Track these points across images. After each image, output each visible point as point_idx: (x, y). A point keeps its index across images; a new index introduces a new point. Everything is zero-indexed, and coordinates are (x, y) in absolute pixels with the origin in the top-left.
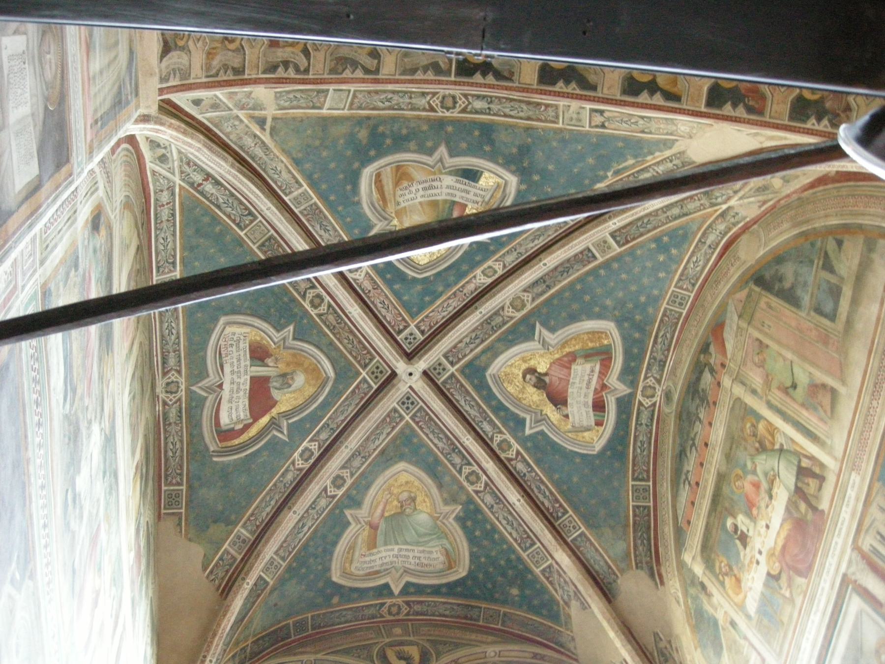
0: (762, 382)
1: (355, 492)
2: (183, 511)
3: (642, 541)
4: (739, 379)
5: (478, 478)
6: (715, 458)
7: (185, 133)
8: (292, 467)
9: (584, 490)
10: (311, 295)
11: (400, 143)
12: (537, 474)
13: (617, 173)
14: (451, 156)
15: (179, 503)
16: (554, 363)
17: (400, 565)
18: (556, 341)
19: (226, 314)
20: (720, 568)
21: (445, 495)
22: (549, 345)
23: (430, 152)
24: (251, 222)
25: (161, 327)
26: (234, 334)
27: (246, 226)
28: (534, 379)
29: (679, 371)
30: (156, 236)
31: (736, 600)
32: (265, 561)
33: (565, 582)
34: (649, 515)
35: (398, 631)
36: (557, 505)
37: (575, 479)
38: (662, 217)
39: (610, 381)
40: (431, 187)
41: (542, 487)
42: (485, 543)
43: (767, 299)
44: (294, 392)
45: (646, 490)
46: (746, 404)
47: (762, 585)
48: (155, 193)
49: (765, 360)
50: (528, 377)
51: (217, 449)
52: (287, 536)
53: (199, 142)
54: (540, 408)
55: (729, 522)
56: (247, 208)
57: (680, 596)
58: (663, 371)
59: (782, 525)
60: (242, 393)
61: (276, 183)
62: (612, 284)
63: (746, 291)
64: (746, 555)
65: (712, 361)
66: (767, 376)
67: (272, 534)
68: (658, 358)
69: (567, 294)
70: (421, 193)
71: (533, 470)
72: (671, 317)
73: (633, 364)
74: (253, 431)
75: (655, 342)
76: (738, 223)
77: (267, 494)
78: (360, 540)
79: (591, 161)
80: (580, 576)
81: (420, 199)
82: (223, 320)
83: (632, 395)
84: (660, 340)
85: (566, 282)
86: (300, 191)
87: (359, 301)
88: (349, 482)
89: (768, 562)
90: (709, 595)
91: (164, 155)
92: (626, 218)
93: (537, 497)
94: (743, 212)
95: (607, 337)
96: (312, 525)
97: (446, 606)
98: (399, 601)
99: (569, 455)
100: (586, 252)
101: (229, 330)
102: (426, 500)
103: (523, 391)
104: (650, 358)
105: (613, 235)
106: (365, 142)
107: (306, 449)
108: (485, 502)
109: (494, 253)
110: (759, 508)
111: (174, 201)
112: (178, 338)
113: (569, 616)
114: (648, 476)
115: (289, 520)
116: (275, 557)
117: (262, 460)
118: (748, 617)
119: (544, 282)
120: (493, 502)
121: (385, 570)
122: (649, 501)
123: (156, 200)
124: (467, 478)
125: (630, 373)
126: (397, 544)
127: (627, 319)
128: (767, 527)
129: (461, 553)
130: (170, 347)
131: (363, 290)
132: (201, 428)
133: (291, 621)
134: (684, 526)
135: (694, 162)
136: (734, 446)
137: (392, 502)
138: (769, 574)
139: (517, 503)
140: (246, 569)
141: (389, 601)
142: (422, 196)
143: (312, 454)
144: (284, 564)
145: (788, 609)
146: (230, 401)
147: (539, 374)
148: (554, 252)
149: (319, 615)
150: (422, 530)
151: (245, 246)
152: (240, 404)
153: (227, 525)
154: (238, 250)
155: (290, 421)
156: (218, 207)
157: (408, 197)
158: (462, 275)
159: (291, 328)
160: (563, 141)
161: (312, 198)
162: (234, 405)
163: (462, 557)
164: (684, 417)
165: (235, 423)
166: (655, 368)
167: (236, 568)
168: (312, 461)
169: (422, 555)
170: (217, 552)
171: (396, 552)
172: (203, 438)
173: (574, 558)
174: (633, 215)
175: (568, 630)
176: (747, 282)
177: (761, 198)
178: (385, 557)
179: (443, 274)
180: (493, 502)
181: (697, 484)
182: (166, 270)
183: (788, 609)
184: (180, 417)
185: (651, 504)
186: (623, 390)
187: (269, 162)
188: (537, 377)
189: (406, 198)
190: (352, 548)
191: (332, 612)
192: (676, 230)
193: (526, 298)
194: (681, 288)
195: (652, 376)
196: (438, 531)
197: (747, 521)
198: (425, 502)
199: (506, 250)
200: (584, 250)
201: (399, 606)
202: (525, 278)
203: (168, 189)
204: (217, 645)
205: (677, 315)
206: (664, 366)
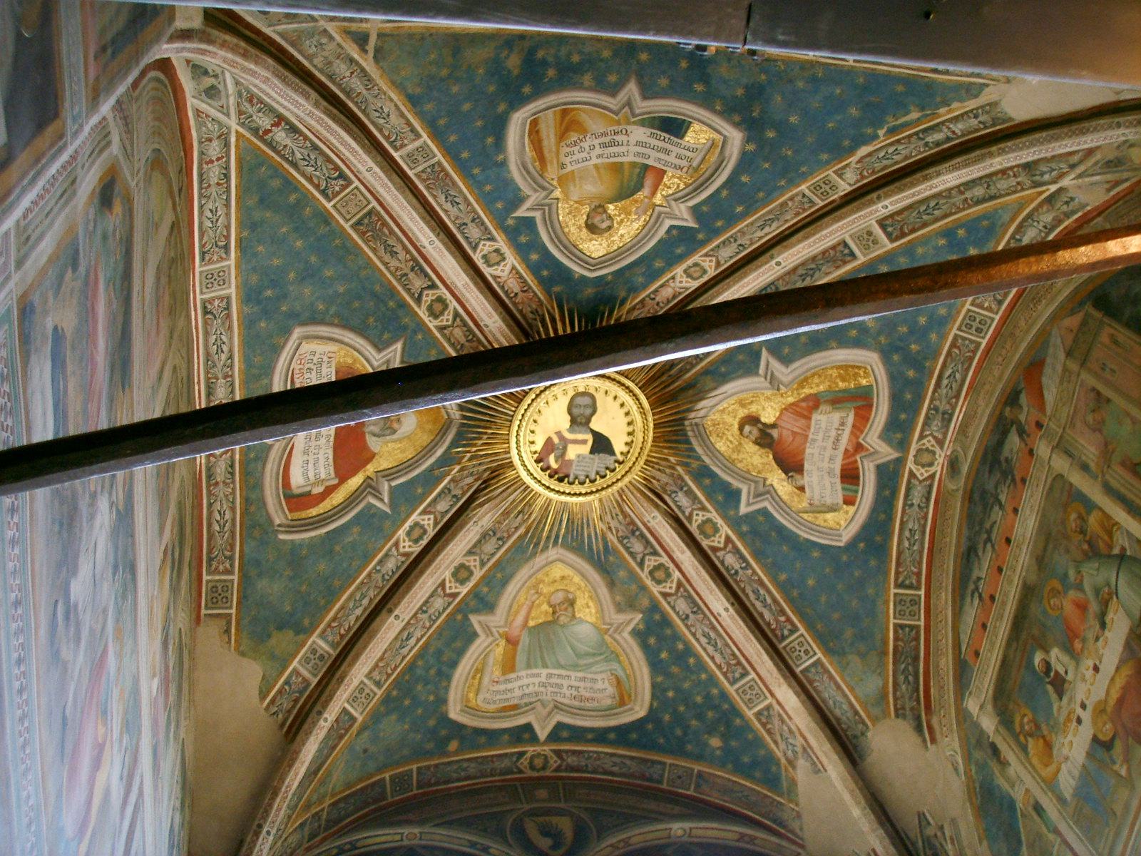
0: (1097, 453)
1: (485, 589)
2: (233, 611)
3: (906, 678)
4: (1062, 447)
5: (668, 575)
6: (1021, 561)
7: (245, 55)
8: (394, 551)
9: (823, 599)
10: (429, 299)
11: (568, 75)
12: (754, 572)
13: (892, 131)
15: (227, 600)
16: (785, 409)
17: (549, 698)
18: (790, 377)
19: (303, 324)
20: (1022, 726)
21: (618, 598)
23: (613, 91)
24: (344, 188)
25: (206, 341)
26: (313, 353)
27: (336, 194)
28: (755, 432)
29: (971, 430)
30: (201, 207)
31: (1043, 774)
32: (352, 687)
33: (791, 731)
34: (917, 639)
35: (542, 793)
36: (783, 619)
38: (958, 199)
39: (868, 439)
40: (613, 144)
41: (762, 592)
42: (675, 669)
43: (1111, 331)
44: (400, 440)
45: (915, 602)
46: (1071, 485)
47: (1084, 754)
48: (200, 143)
49: (1103, 421)
50: (747, 428)
51: (284, 521)
52: (385, 651)
53: (267, 68)
54: (763, 475)
55: (1038, 657)
56: (337, 168)
57: (960, 761)
58: (947, 427)
59: (1118, 669)
60: (323, 441)
61: (380, 131)
63: (1078, 318)
64: (1060, 708)
65: (1022, 418)
66: (1106, 444)
67: (365, 647)
68: (941, 409)
70: (598, 151)
71: (748, 566)
72: (964, 349)
73: (903, 416)
74: (338, 497)
75: (938, 384)
76: (1074, 212)
77: (357, 589)
78: (491, 661)
79: (853, 111)
80: (813, 725)
81: (595, 161)
82: (298, 332)
83: (900, 462)
84: (945, 382)
86: (417, 144)
87: (501, 309)
88: (478, 574)
89: (1094, 723)
90: (1004, 764)
91: (213, 87)
92: (902, 199)
93: (753, 605)
94: (1081, 197)
95: (866, 375)
96: (422, 636)
97: (615, 759)
98: (546, 749)
99: (802, 547)
100: (841, 248)
101: (306, 347)
102: (591, 604)
103: (738, 449)
104: (929, 409)
105: (882, 223)
106: (516, 72)
107: (416, 524)
108: (676, 610)
109: (703, 243)
110: (1084, 640)
111: (228, 156)
112: (231, 357)
113: (793, 783)
114: (919, 582)
115: (389, 629)
116: (366, 681)
117: (350, 539)
118: (1061, 800)
120: (688, 611)
121: (526, 705)
122: (919, 619)
123: (202, 153)
124: (651, 573)
125: (898, 430)
126: (545, 666)
127: (897, 349)
128: (1096, 669)
129: (639, 684)
130: (218, 371)
131: (506, 293)
132: (262, 490)
133: (387, 776)
134: (970, 659)
135: (1011, 119)
136: (1051, 546)
137: (539, 606)
138: (1095, 739)
139: (724, 614)
140: (323, 698)
141: (531, 750)
142: (599, 156)
143: (425, 532)
144: (379, 693)
145: (1123, 794)
146: (306, 452)
147: (765, 425)
148: (793, 245)
149: (428, 767)
150: (583, 648)
151: (334, 224)
152: (321, 456)
153: (297, 633)
154: (323, 230)
155: (394, 484)
156: (294, 165)
157: (578, 156)
158: (654, 275)
159: (399, 346)
160: (814, 80)
161: (435, 156)
162: (311, 458)
163: (640, 689)
164: (976, 496)
165: (312, 485)
166: (936, 424)
167: (309, 697)
168: (424, 542)
169: (582, 684)
170: (281, 673)
171: (543, 679)
172: (264, 504)
173: (803, 696)
174: (914, 195)
175: (791, 801)
176: (1081, 304)
177: (1109, 177)
178: (528, 686)
179: (627, 274)
180: (688, 611)
181: (992, 598)
182: (215, 258)
183: (1123, 794)
184: (232, 474)
185: (922, 623)
186: (887, 453)
187: (371, 99)
188: (760, 430)
189: (575, 157)
190: (480, 671)
191: (449, 763)
192: (979, 219)
194: (981, 307)
195: (931, 435)
196: (605, 652)
197: (1065, 658)
198: (588, 607)
199: (722, 239)
200: (839, 244)
201: (546, 757)
202: (748, 283)
203: (219, 137)
204: (279, 810)
205: (972, 347)
206: (950, 420)
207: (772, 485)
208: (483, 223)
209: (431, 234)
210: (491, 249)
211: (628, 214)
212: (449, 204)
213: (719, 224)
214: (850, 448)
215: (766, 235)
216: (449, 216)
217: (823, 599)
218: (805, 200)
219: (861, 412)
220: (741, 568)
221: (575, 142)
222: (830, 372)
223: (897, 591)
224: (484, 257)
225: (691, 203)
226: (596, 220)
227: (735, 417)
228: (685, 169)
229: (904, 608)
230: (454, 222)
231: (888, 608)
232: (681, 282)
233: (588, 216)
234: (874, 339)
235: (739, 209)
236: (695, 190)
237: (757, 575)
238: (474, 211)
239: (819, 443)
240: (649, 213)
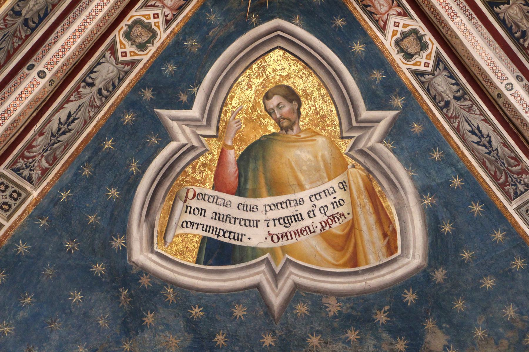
14: (258, 287)
40: (286, 221)
70: (303, 209)
81: (305, 195)
106: (430, 324)
119: (26, 22)
142: (300, 202)
157: (326, 201)
161: (517, 209)
189: (330, 199)
208: (433, 99)
209: (512, 99)
210: (417, 59)
211: (249, 120)
212: (484, 131)
213: (128, 118)
215: (61, 107)
216: (482, 113)
218: (26, 173)
221: (333, 221)
224: (424, 46)
225: (172, 146)
226: (287, 108)
228: (191, 195)
230: (474, 102)
232: (156, 16)
233: (299, 113)
235: (108, 144)
236: (172, 167)
238: (448, 119)
240: (223, 124)
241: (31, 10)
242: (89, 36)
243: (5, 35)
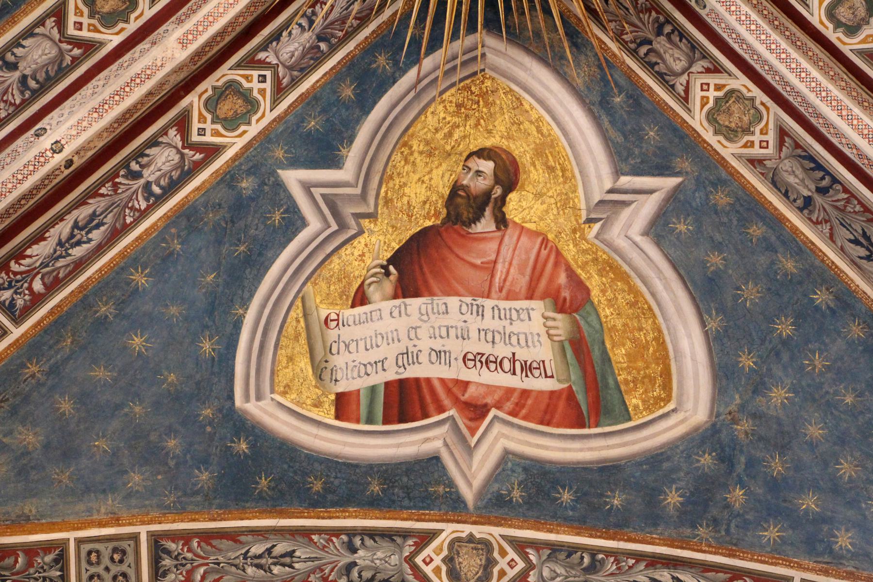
9: (101, 374)
12: (143, 214)
16: (545, 241)
18: (622, 243)
22: (607, 223)
28: (481, 184)
37: (137, 342)
39: (497, 428)
41: (96, 235)
50: (487, 166)
62: (849, 400)
69: (790, 265)
85: (833, 255)
93: (60, 218)
104: (593, 552)
120: (26, 68)
127: (726, 459)
147: (502, 200)
180: (26, 68)
188: (487, 194)
193: (756, 138)
195: (530, 566)
207: (361, 232)
214: (472, 391)
217: (101, 374)
219: (562, 404)
220: (148, 185)
222: (647, 325)
223: (143, 538)
227: (509, 137)
229: (106, 561)
231: (101, 525)
234: (742, 407)
237: (137, 222)
239: (474, 324)
241: (803, 181)
242: (849, 94)
243: (842, 224)
